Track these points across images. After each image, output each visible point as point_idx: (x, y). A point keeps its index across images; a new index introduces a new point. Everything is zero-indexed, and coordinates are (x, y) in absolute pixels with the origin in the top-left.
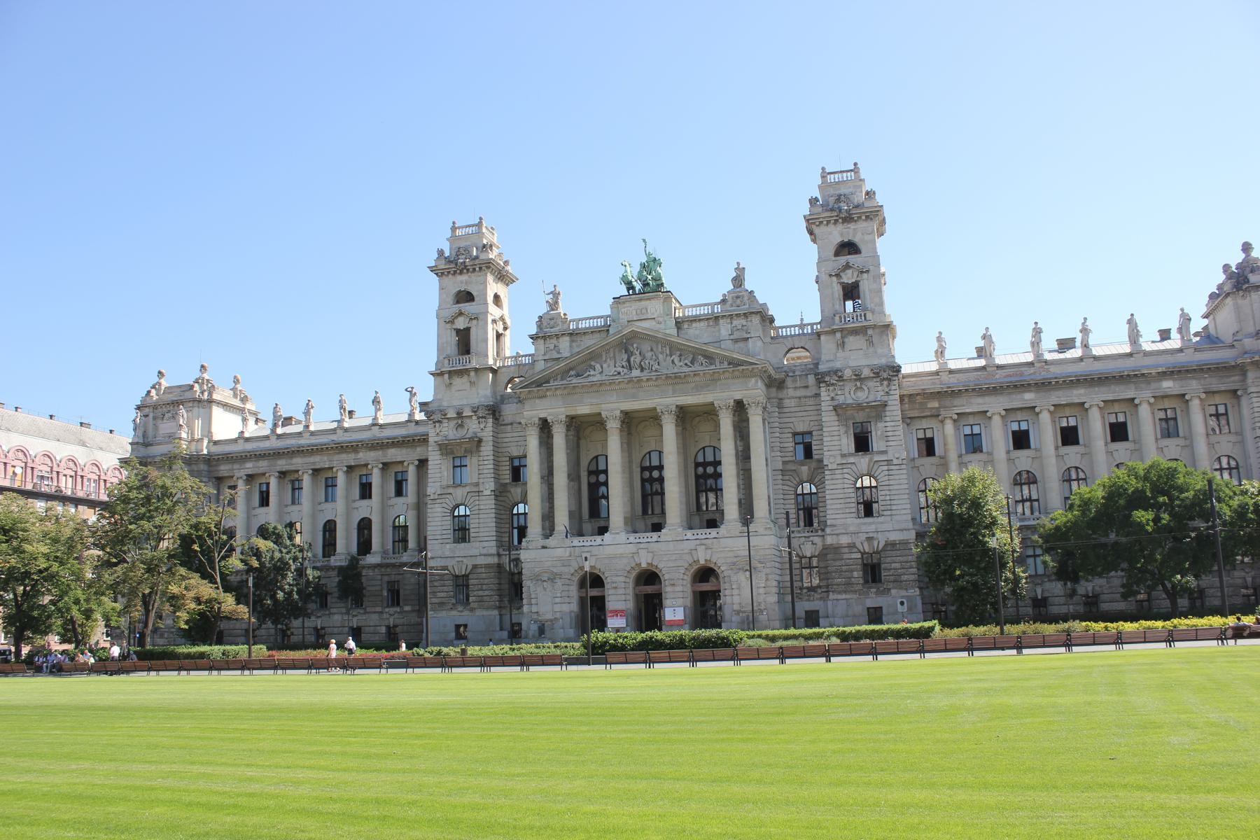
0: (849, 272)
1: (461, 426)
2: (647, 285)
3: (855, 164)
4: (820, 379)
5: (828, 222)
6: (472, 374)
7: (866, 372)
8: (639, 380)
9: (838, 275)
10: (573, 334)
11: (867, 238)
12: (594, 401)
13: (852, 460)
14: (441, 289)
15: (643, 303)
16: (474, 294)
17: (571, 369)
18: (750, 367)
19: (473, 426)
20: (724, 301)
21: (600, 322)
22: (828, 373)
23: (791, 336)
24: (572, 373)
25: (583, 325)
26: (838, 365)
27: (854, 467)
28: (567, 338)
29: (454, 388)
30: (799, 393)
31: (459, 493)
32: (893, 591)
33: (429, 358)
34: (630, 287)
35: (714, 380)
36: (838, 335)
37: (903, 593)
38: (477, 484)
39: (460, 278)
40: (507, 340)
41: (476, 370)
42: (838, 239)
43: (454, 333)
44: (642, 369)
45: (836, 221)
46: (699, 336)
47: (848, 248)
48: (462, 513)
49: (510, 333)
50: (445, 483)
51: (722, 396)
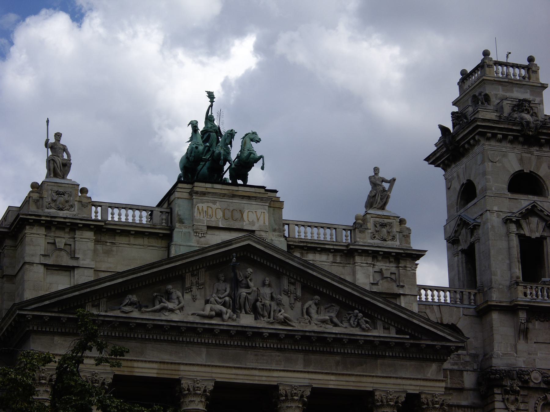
0: (534, 220)
3: (531, 59)
5: (505, 137)
10: (105, 231)
12: (166, 358)
17: (131, 292)
20: (359, 226)
22: (508, 374)
23: (440, 305)
24: (134, 298)
25: (114, 216)
26: (521, 363)
28: (90, 235)
35: (372, 352)
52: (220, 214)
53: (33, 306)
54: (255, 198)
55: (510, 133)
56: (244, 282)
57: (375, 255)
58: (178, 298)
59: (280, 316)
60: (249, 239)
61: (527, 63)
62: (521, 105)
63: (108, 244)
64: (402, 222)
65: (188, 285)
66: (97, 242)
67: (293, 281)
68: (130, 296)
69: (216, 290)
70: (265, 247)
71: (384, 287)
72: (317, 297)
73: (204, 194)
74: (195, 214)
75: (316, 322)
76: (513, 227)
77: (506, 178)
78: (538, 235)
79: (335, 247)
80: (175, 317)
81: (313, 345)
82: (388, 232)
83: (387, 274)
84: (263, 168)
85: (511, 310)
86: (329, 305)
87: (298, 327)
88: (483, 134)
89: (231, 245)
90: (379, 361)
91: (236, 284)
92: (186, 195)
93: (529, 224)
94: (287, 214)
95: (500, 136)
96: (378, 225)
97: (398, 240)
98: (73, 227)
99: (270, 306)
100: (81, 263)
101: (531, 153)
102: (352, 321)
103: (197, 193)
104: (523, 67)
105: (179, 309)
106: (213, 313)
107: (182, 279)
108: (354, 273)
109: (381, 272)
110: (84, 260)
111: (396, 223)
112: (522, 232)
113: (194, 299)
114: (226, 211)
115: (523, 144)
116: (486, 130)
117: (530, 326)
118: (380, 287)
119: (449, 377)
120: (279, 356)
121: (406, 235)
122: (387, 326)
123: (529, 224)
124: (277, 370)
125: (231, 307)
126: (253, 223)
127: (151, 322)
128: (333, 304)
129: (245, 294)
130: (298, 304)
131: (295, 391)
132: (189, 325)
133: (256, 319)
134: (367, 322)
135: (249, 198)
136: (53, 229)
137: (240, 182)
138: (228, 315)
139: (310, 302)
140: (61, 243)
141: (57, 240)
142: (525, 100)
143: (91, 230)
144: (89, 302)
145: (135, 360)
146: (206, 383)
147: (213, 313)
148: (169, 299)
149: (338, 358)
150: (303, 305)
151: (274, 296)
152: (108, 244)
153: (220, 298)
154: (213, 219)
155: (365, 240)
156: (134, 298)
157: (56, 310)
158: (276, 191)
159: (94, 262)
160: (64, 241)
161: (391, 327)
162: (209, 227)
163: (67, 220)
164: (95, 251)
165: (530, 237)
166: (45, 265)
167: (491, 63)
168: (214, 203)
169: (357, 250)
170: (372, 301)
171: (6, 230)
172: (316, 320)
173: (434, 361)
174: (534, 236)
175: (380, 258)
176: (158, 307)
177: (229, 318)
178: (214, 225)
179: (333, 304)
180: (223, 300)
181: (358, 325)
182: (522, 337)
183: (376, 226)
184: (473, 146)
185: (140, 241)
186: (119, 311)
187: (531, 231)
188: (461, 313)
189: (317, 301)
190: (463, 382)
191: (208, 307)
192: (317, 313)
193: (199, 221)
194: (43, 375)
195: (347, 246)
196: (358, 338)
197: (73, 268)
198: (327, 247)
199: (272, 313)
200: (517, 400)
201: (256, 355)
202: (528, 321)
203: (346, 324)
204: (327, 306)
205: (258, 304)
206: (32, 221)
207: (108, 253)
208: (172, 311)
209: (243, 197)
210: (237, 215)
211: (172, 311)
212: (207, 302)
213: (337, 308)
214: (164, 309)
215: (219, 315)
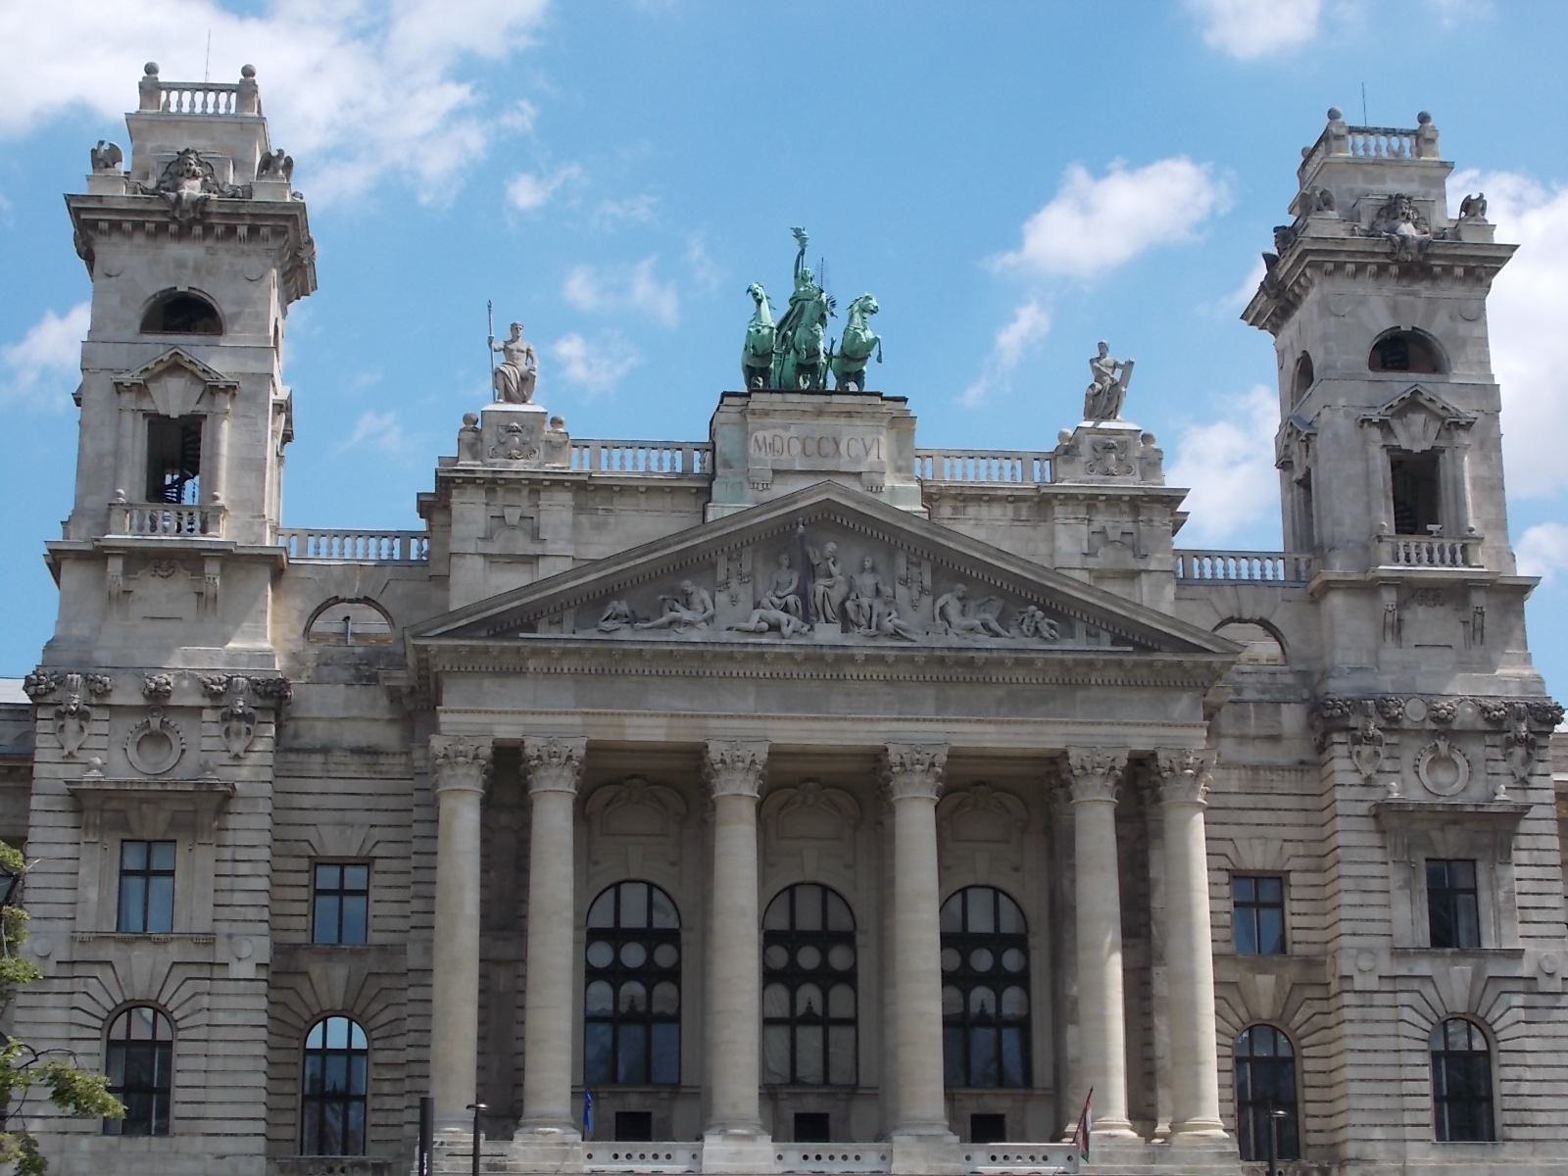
0: (1418, 419)
1: (157, 738)
3: (1423, 118)
4: (1328, 720)
5: (1360, 268)
6: (212, 568)
7: (1467, 715)
8: (843, 658)
9: (1384, 425)
10: (591, 492)
11: (1463, 329)
13: (1423, 967)
15: (826, 421)
16: (225, 308)
18: (1187, 659)
19: (199, 750)
20: (1067, 451)
21: (665, 464)
22: (1357, 705)
23: (1237, 583)
24: (622, 607)
26: (1386, 683)
27: (1429, 991)
28: (565, 497)
30: (1254, 754)
31: (142, 968)
33: (48, 505)
35: (1069, 682)
36: (1389, 598)
38: (208, 940)
39: (175, 250)
41: (229, 558)
42: (1380, 321)
43: (142, 428)
44: (847, 623)
45: (1382, 269)
47: (1400, 351)
48: (141, 1032)
49: (334, 454)
50: (87, 923)
51: (1094, 733)
52: (796, 447)
53: (439, 631)
55: (1371, 260)
56: (822, 566)
57: (1091, 502)
58: (703, 602)
59: (888, 626)
60: (827, 491)
61: (1415, 125)
62: (1393, 208)
63: (600, 512)
64: (1147, 438)
65: (721, 576)
66: (579, 509)
67: (914, 559)
68: (615, 603)
69: (775, 584)
70: (858, 503)
72: (961, 587)
73: (766, 413)
74: (751, 451)
75: (959, 632)
76: (1376, 434)
77: (1366, 346)
78: (1428, 447)
79: (1015, 493)
80: (695, 636)
81: (953, 673)
82: (1119, 459)
84: (879, 360)
85: (1369, 588)
86: (986, 599)
87: (921, 641)
89: (795, 502)
90: (1080, 695)
91: (810, 571)
92: (735, 417)
93: (1407, 427)
94: (923, 439)
95: (1350, 267)
96: (1098, 448)
97: (1138, 472)
98: (535, 486)
99: (871, 607)
100: (551, 548)
102: (1024, 627)
103: (753, 412)
104: (1407, 134)
105: (706, 621)
106: (765, 625)
107: (713, 566)
108: (1052, 537)
109: (1103, 532)
110: (554, 542)
112: (1395, 443)
113: (734, 601)
114: (808, 442)
115: (1400, 277)
116: (1321, 259)
117: (1407, 615)
118: (1100, 559)
119: (1253, 715)
120: (889, 694)
121: (1153, 462)
122: (1093, 632)
123: (1407, 427)
124: (885, 720)
125: (801, 612)
126: (857, 460)
127: (648, 647)
128: (993, 597)
129: (822, 588)
130: (927, 600)
131: (917, 756)
132: (717, 648)
133: (845, 630)
134: (1052, 626)
135: (849, 414)
137: (853, 387)
138: (791, 626)
140: (513, 516)
141: (507, 511)
142: (1400, 197)
144: (543, 617)
145: (625, 715)
146: (753, 748)
147: (765, 625)
148: (688, 605)
149: (1000, 692)
150: (934, 601)
151: (881, 587)
152: (600, 512)
153: (780, 598)
154: (783, 457)
155: (1075, 479)
156: (622, 607)
157: (484, 633)
158: (905, 400)
159: (569, 544)
160: (518, 512)
161: (1101, 632)
162: (775, 472)
163: (522, 476)
164: (575, 526)
165: (1409, 451)
166: (485, 555)
167: (1343, 131)
168: (786, 428)
169: (1056, 495)
170: (1059, 588)
171: (431, 499)
173: (1183, 688)
174: (1417, 449)
175: (1101, 506)
176: (664, 620)
177: (794, 632)
179: (993, 597)
180: (784, 601)
182: (1389, 637)
183: (1095, 450)
184: (1306, 289)
185: (657, 502)
186: (595, 630)
187: (1413, 439)
188: (1279, 599)
189: (960, 594)
190: (1280, 723)
191: (756, 615)
192: (963, 613)
194: (461, 748)
195: (1037, 489)
196: (1033, 655)
197: (537, 557)
198: (1000, 493)
199: (874, 619)
200: (1377, 754)
201: (848, 694)
202: (1401, 605)
203: (1014, 632)
204: (979, 602)
205: (848, 604)
206: (460, 481)
207: (599, 527)
208: (688, 624)
209: (838, 414)
210: (828, 447)
211: (688, 624)
212: (757, 605)
213: (998, 603)
215: (775, 627)
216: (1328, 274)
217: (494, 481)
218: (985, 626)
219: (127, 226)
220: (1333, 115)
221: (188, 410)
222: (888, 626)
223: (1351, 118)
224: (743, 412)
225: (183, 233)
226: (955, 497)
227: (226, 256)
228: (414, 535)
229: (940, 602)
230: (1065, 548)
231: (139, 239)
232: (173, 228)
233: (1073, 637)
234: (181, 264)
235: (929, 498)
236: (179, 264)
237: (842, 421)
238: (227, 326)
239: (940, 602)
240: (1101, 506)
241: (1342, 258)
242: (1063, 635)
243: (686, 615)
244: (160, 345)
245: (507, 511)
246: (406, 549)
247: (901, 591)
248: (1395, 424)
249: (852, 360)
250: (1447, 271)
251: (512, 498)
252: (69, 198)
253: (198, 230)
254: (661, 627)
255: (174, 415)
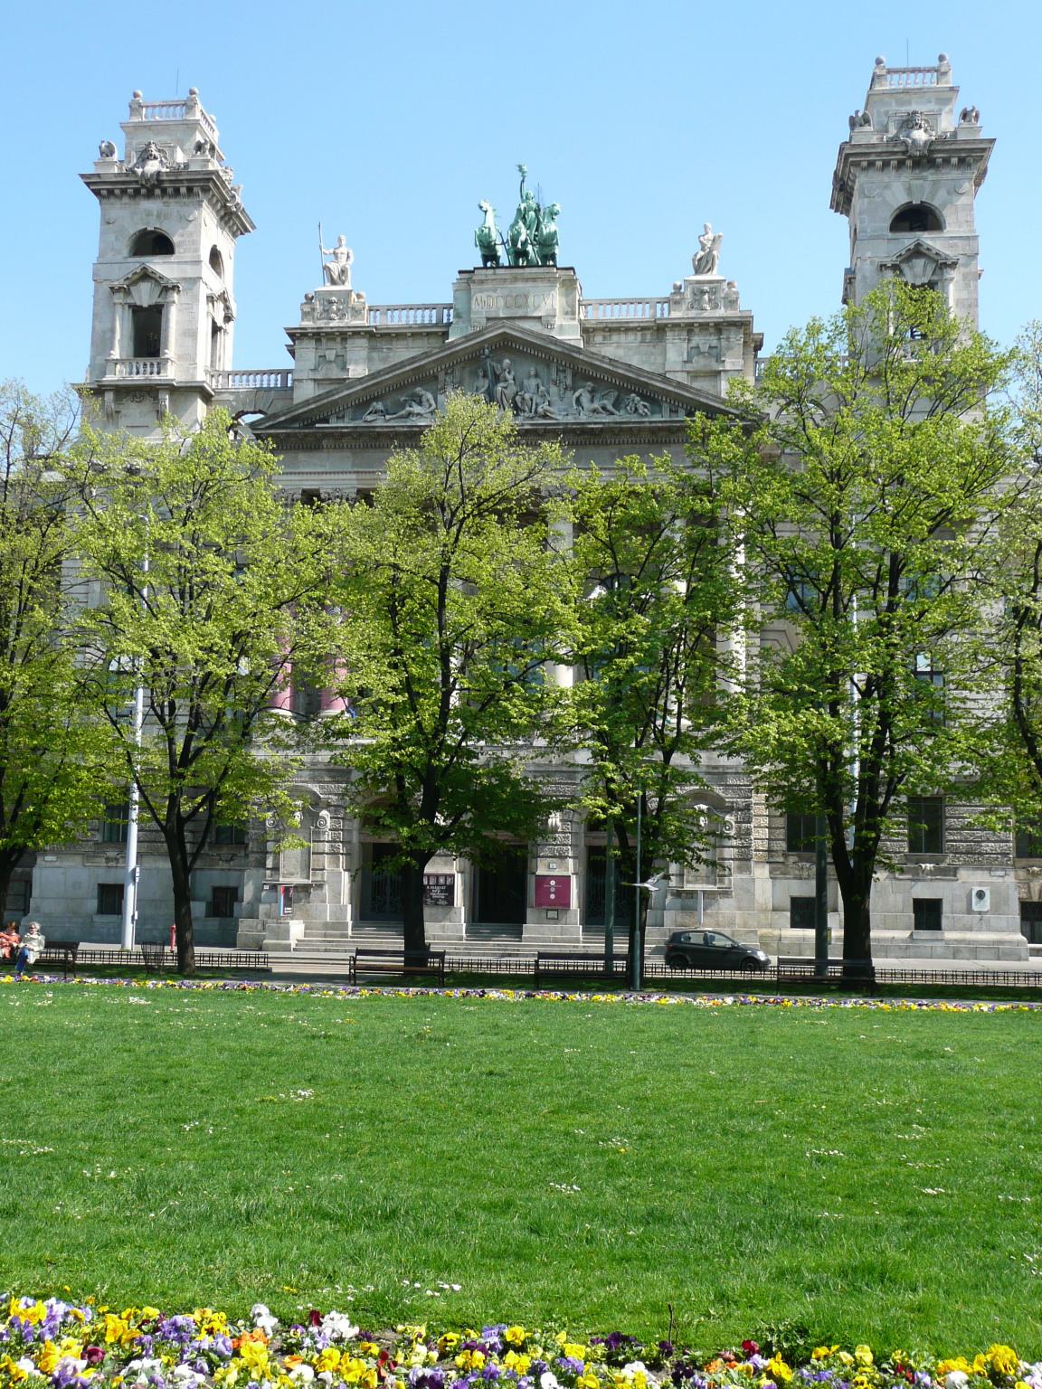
0: (919, 263)
2: (530, 253)
3: (941, 58)
5: (886, 164)
9: (895, 267)
10: (375, 337)
14: (107, 222)
15: (520, 285)
17: (376, 399)
21: (429, 317)
24: (379, 406)
28: (363, 342)
29: (123, 422)
32: (963, 874)
34: (490, 255)
37: (982, 876)
40: (227, 340)
41: (173, 389)
43: (128, 314)
45: (901, 164)
46: (624, 353)
47: (917, 217)
52: (501, 302)
54: (542, 279)
57: (689, 328)
66: (372, 349)
71: (699, 363)
72: (590, 384)
73: (482, 282)
83: (704, 348)
87: (561, 419)
88: (857, 164)
91: (497, 378)
93: (911, 268)
95: (879, 164)
98: (344, 336)
101: (925, 179)
108: (664, 352)
111: (725, 286)
121: (732, 302)
123: (911, 268)
130: (569, 393)
135: (534, 280)
136: (324, 340)
139: (580, 391)
140: (331, 355)
141: (327, 353)
142: (915, 113)
143: (363, 337)
148: (420, 403)
166: (315, 380)
168: (495, 291)
172: (585, 410)
175: (697, 330)
176: (403, 412)
178: (493, 315)
181: (636, 409)
187: (915, 276)
192: (592, 401)
193: (478, 312)
205: (518, 399)
209: (527, 280)
214: (410, 414)
216: (864, 169)
217: (318, 334)
218: (604, 408)
219: (117, 192)
220: (879, 62)
221: (153, 302)
222: (540, 410)
223: (888, 64)
224: (469, 282)
225: (150, 194)
226: (603, 330)
227: (174, 206)
228: (289, 371)
229: (577, 394)
230: (673, 360)
231: (126, 200)
232: (143, 191)
233: (661, 412)
234: (149, 214)
235: (587, 331)
236: (149, 214)
237: (530, 284)
238: (177, 250)
239: (577, 394)
240: (697, 330)
241: (872, 158)
242: (653, 413)
243: (417, 409)
244: (135, 264)
245: (327, 353)
246: (285, 380)
247: (553, 389)
248: (905, 267)
249: (547, 247)
250: (946, 161)
251: (331, 344)
252: (82, 176)
253: (158, 192)
254: (401, 417)
255: (145, 305)
